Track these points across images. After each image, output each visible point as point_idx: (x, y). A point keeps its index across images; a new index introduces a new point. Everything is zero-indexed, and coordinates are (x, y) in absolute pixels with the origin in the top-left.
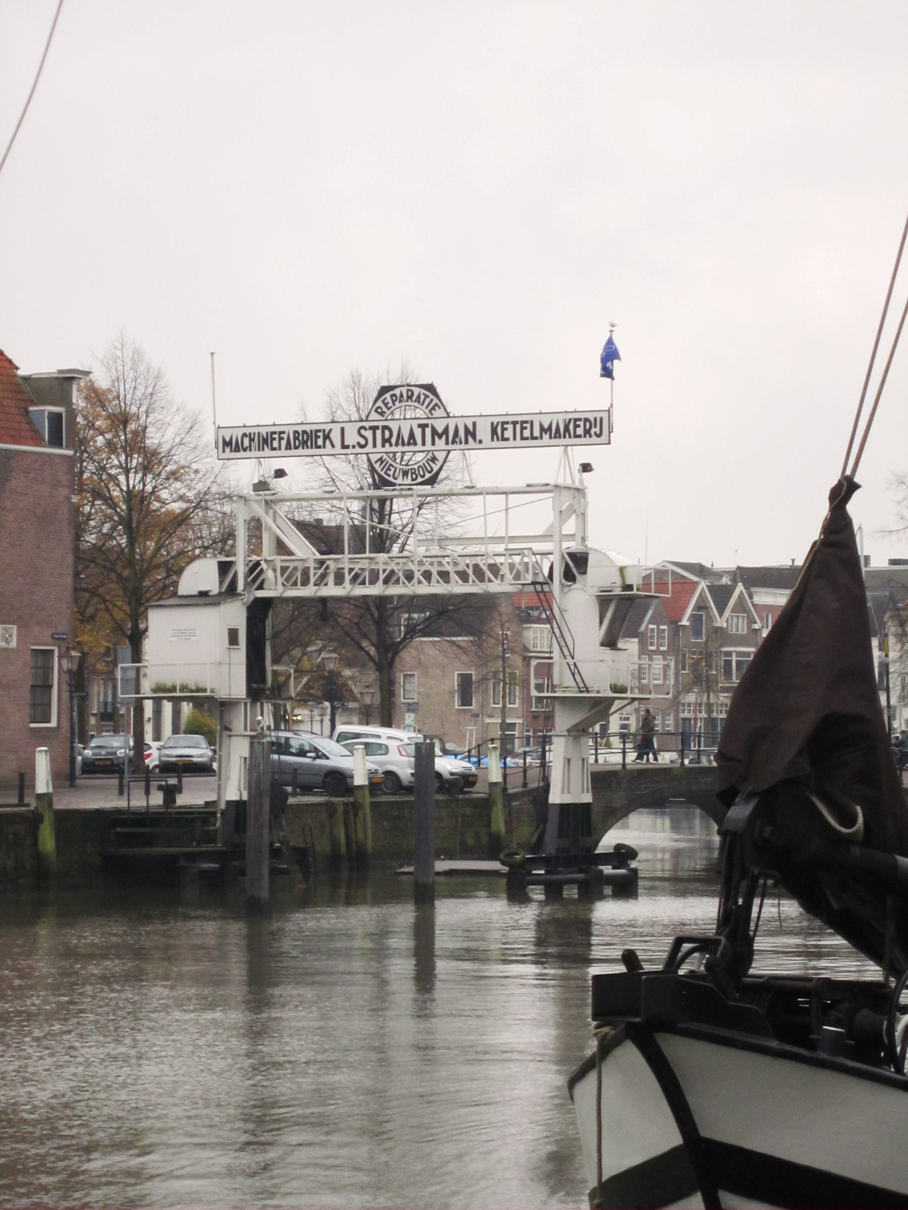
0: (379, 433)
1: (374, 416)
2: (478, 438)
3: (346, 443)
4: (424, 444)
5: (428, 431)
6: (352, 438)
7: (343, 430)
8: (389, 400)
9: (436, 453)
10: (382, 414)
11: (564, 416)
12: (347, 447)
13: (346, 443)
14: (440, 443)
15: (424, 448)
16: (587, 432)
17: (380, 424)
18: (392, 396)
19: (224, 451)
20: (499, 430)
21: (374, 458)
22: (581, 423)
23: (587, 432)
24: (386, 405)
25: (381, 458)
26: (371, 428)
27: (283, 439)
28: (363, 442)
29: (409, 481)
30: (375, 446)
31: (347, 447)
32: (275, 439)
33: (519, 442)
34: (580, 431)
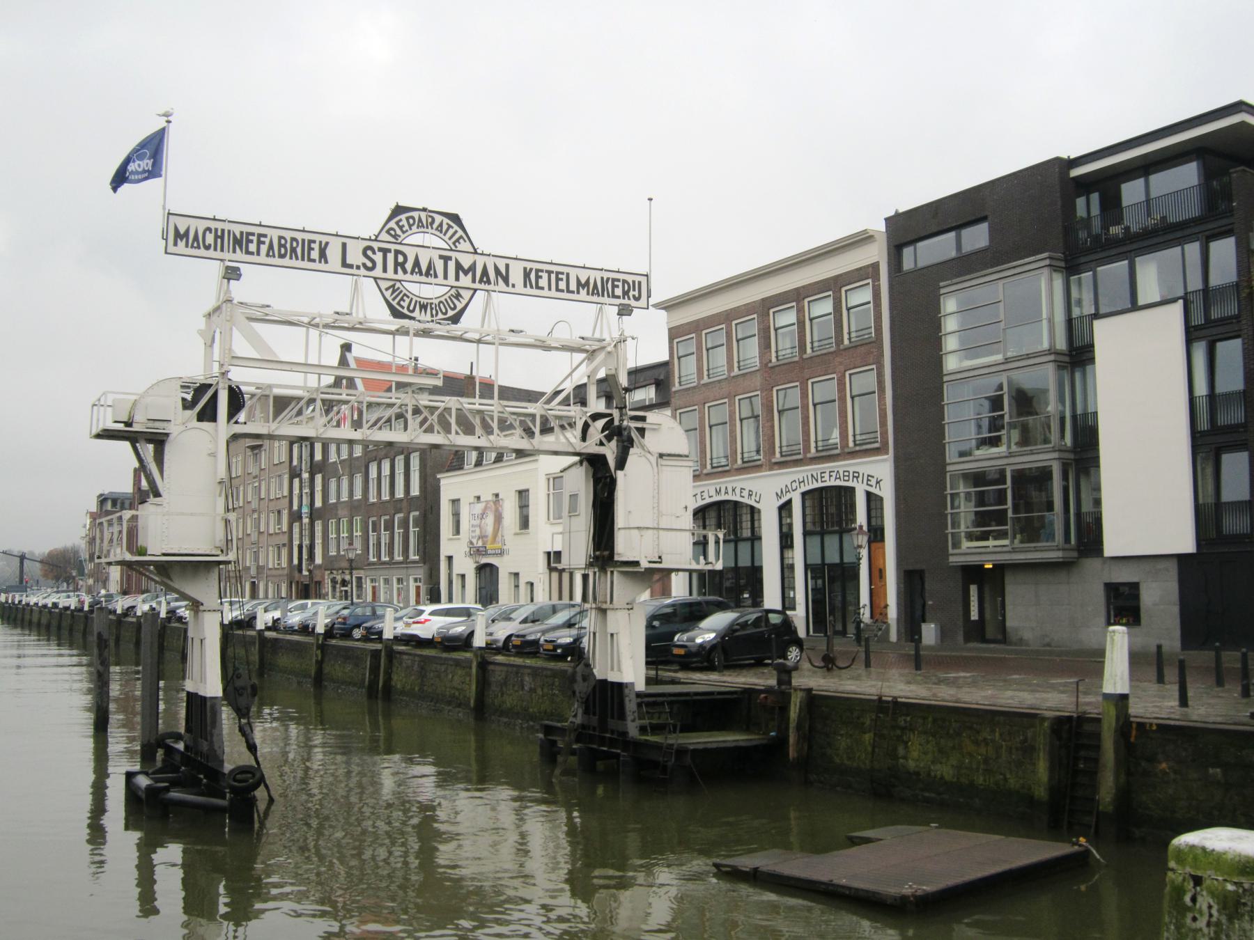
0: (391, 257)
1: (384, 236)
2: (511, 282)
3: (348, 261)
4: (446, 277)
5: (451, 265)
6: (355, 257)
7: (344, 245)
8: (404, 222)
9: (461, 291)
10: (396, 236)
11: (606, 275)
12: (351, 266)
13: (348, 261)
14: (465, 280)
15: (445, 282)
17: (393, 247)
18: (407, 219)
19: (175, 244)
20: (533, 276)
21: (384, 285)
22: (620, 284)
23: (626, 293)
24: (401, 228)
25: (393, 286)
26: (380, 249)
27: (264, 243)
28: (369, 264)
29: (428, 318)
30: (385, 270)
31: (351, 266)
32: (252, 241)
33: (553, 293)
34: (618, 292)
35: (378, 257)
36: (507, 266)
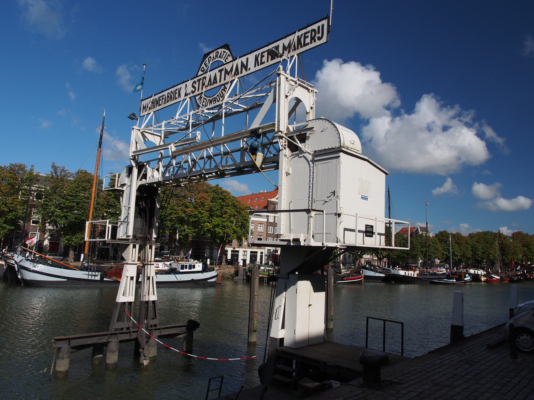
0: (201, 81)
5: (223, 72)
8: (207, 62)
16: (313, 39)
22: (309, 34)
23: (313, 39)
34: (308, 40)
35: (196, 86)
36: (247, 59)
